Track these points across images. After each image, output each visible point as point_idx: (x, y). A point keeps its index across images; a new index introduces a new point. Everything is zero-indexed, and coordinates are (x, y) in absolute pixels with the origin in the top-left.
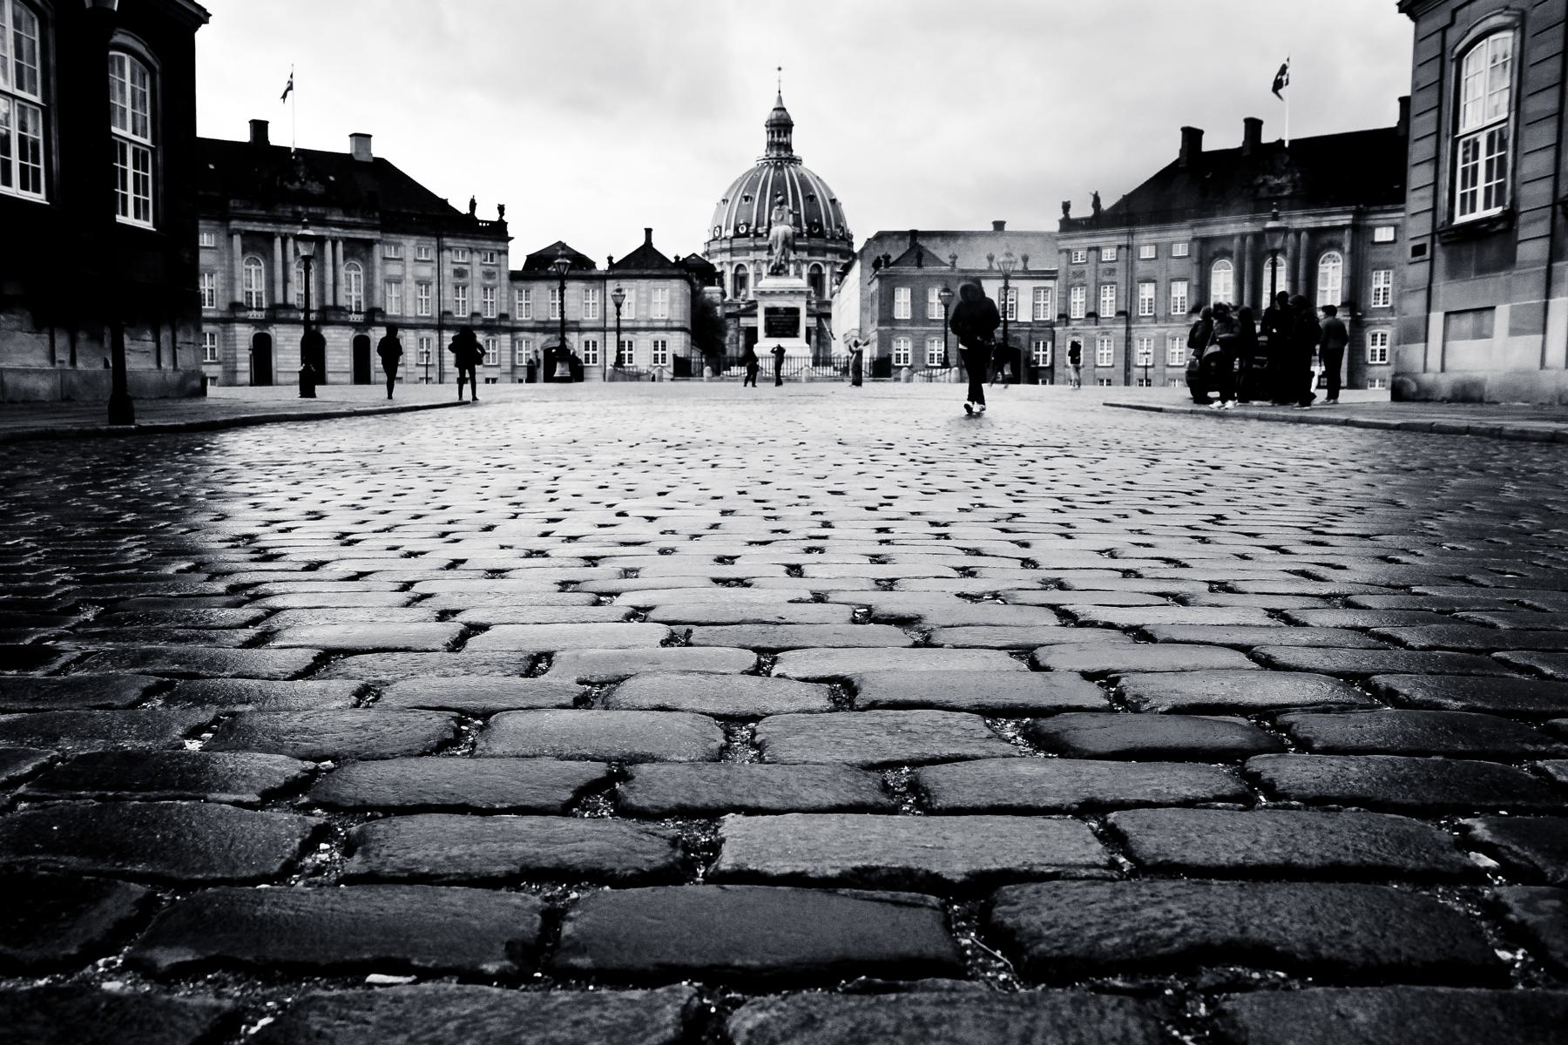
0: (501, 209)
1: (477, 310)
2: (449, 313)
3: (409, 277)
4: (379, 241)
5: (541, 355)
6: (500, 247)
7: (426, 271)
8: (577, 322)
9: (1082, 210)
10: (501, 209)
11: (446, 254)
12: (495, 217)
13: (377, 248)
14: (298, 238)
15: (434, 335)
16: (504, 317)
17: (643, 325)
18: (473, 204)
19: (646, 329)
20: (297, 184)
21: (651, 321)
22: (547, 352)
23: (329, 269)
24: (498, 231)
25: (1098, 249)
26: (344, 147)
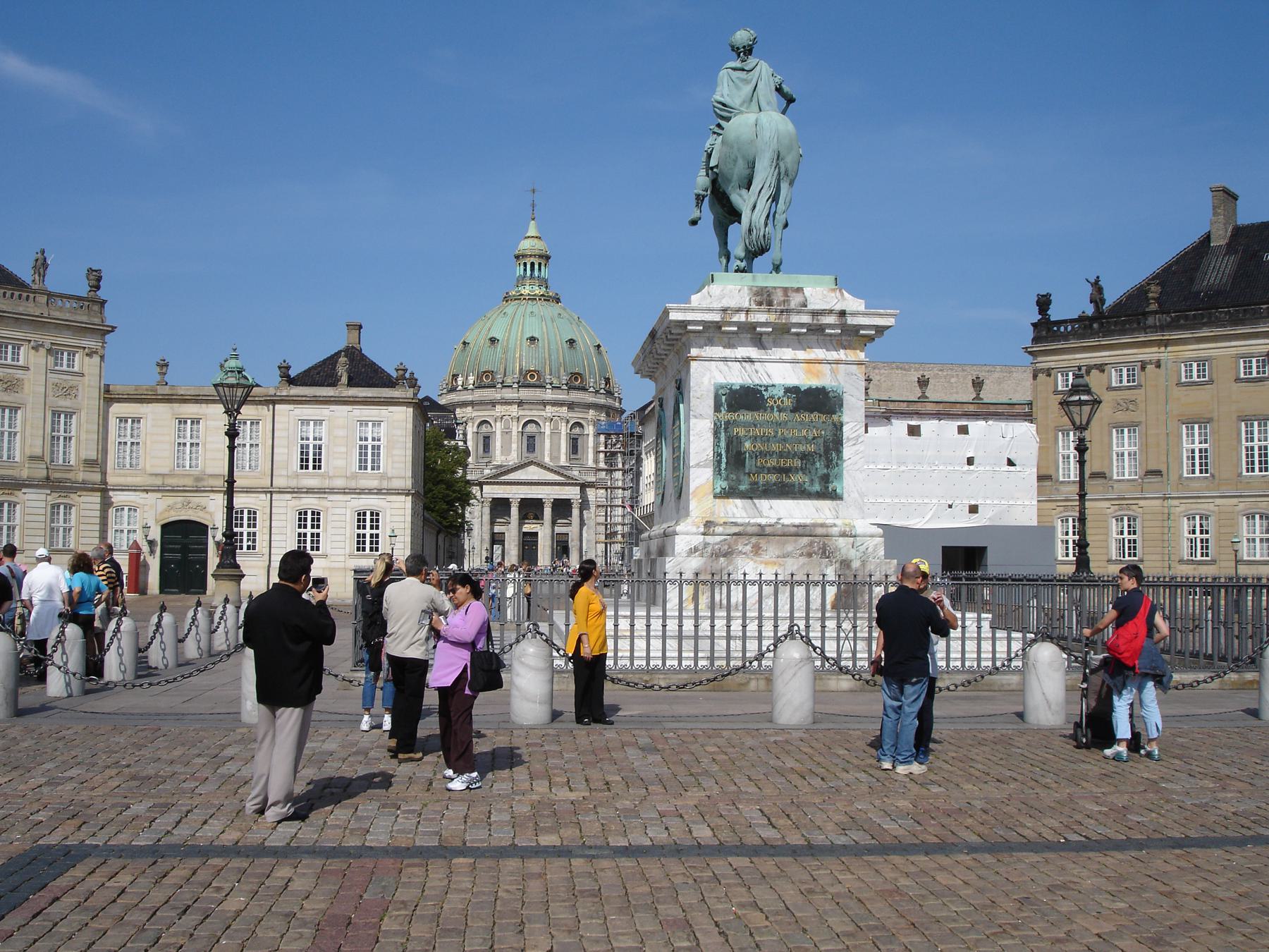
0: (96, 279)
5: (156, 534)
9: (1071, 304)
10: (96, 279)
12: (83, 289)
16: (90, 463)
17: (339, 483)
19: (344, 491)
22: (167, 528)
25: (1101, 368)
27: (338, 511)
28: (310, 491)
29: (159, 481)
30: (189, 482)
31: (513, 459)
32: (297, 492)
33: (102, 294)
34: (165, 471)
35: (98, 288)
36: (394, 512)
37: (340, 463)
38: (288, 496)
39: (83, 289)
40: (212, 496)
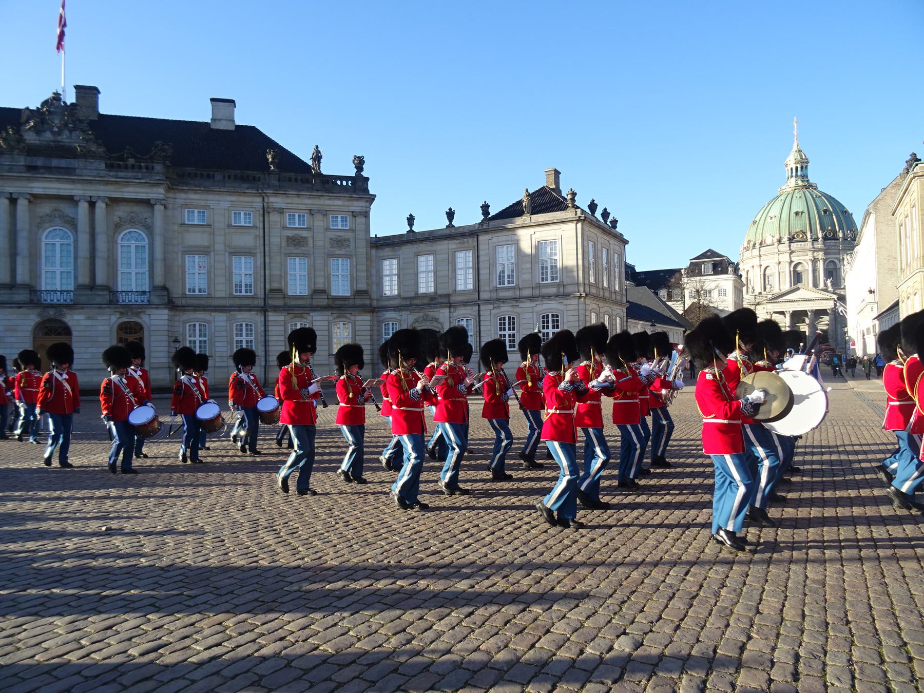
0: (359, 163)
1: (320, 286)
2: (279, 291)
3: (219, 247)
4: (158, 201)
6: (357, 206)
7: (247, 240)
8: (448, 296)
10: (359, 163)
11: (274, 217)
12: (352, 172)
13: (159, 208)
14: (34, 198)
15: (256, 319)
16: (358, 293)
17: (526, 293)
18: (317, 157)
20: (48, 136)
21: (539, 286)
23: (84, 238)
24: (358, 187)
26: (203, 114)
27: (527, 315)
28: (506, 300)
29: (408, 303)
30: (426, 301)
31: (786, 287)
32: (496, 301)
33: (364, 174)
34: (412, 294)
35: (362, 170)
36: (569, 313)
37: (527, 277)
38: (491, 307)
39: (352, 172)
40: (442, 310)
